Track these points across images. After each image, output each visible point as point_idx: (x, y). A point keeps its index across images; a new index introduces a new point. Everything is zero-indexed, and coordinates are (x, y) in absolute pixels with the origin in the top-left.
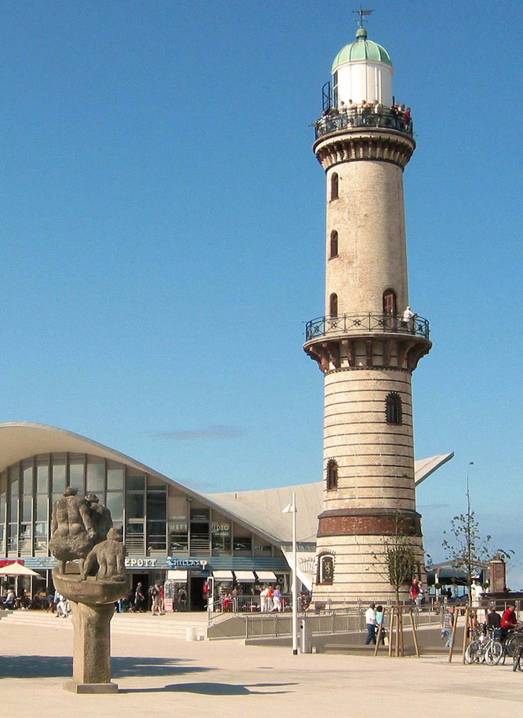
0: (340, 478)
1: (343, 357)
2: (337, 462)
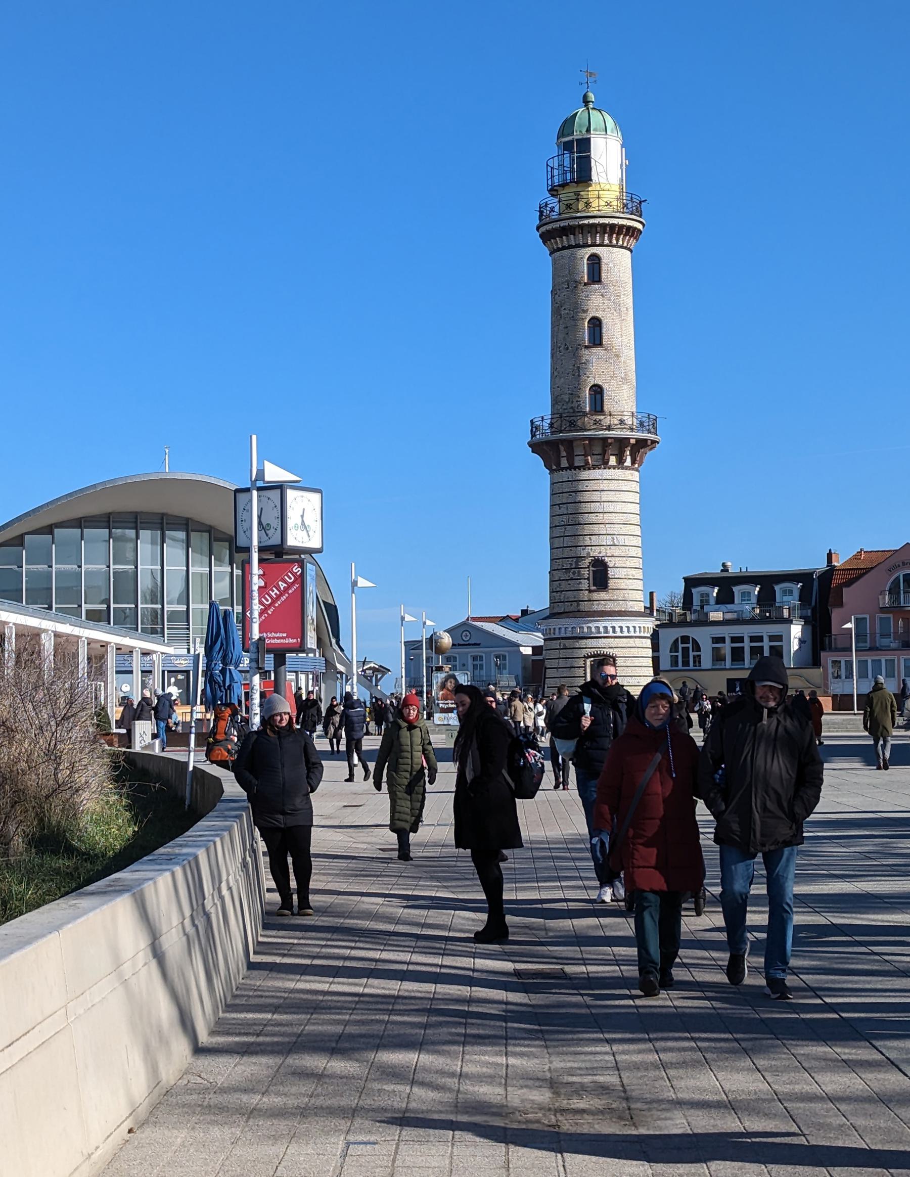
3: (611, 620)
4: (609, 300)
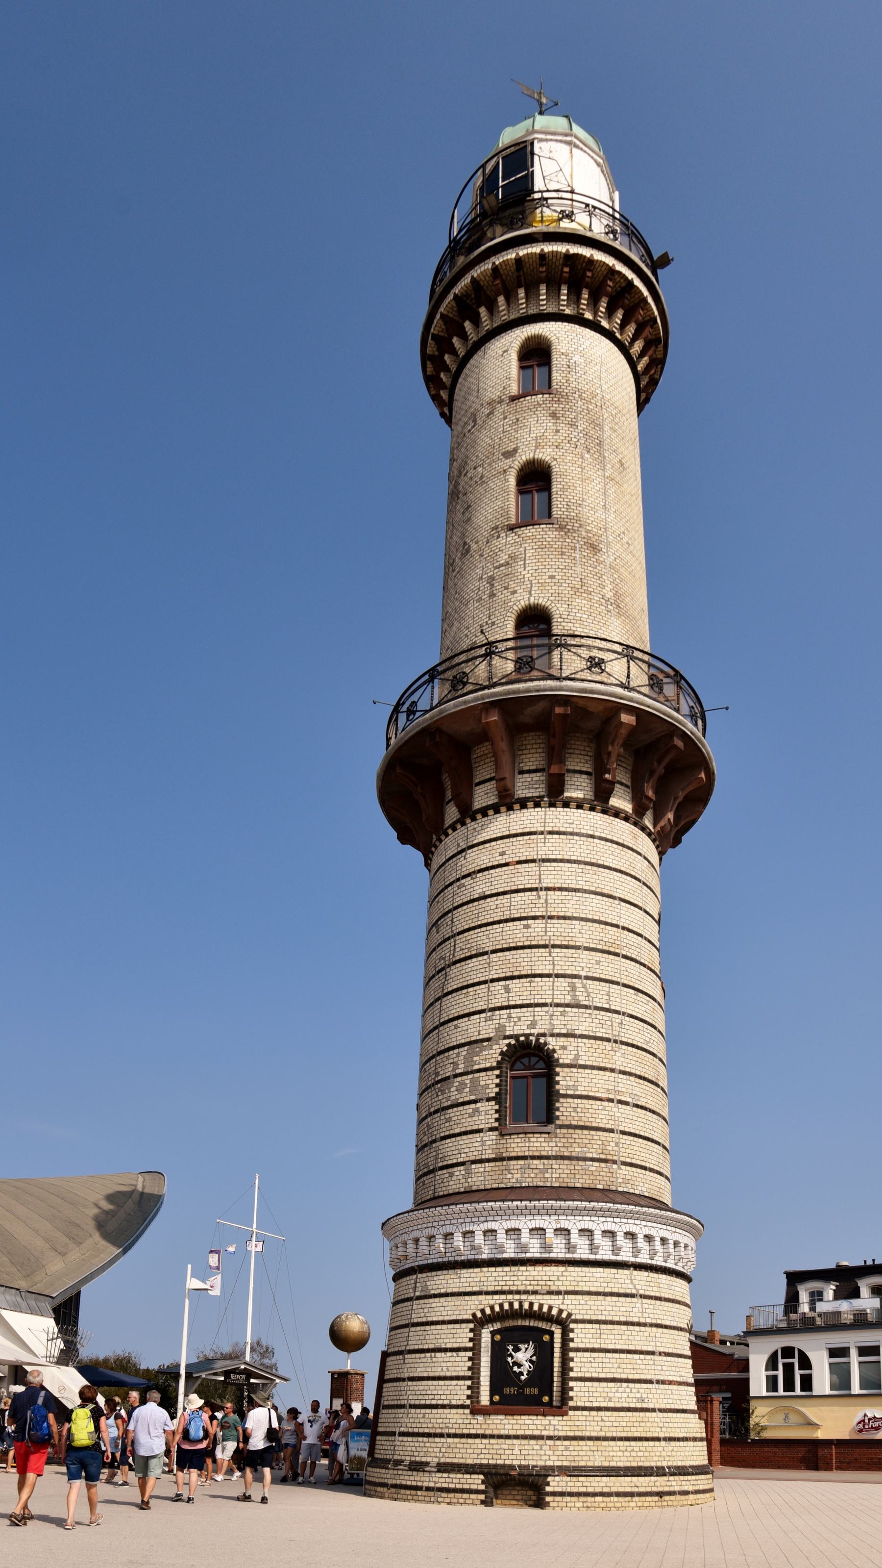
0: (566, 1096)
2: (554, 1051)
3: (556, 1211)
4: (572, 425)
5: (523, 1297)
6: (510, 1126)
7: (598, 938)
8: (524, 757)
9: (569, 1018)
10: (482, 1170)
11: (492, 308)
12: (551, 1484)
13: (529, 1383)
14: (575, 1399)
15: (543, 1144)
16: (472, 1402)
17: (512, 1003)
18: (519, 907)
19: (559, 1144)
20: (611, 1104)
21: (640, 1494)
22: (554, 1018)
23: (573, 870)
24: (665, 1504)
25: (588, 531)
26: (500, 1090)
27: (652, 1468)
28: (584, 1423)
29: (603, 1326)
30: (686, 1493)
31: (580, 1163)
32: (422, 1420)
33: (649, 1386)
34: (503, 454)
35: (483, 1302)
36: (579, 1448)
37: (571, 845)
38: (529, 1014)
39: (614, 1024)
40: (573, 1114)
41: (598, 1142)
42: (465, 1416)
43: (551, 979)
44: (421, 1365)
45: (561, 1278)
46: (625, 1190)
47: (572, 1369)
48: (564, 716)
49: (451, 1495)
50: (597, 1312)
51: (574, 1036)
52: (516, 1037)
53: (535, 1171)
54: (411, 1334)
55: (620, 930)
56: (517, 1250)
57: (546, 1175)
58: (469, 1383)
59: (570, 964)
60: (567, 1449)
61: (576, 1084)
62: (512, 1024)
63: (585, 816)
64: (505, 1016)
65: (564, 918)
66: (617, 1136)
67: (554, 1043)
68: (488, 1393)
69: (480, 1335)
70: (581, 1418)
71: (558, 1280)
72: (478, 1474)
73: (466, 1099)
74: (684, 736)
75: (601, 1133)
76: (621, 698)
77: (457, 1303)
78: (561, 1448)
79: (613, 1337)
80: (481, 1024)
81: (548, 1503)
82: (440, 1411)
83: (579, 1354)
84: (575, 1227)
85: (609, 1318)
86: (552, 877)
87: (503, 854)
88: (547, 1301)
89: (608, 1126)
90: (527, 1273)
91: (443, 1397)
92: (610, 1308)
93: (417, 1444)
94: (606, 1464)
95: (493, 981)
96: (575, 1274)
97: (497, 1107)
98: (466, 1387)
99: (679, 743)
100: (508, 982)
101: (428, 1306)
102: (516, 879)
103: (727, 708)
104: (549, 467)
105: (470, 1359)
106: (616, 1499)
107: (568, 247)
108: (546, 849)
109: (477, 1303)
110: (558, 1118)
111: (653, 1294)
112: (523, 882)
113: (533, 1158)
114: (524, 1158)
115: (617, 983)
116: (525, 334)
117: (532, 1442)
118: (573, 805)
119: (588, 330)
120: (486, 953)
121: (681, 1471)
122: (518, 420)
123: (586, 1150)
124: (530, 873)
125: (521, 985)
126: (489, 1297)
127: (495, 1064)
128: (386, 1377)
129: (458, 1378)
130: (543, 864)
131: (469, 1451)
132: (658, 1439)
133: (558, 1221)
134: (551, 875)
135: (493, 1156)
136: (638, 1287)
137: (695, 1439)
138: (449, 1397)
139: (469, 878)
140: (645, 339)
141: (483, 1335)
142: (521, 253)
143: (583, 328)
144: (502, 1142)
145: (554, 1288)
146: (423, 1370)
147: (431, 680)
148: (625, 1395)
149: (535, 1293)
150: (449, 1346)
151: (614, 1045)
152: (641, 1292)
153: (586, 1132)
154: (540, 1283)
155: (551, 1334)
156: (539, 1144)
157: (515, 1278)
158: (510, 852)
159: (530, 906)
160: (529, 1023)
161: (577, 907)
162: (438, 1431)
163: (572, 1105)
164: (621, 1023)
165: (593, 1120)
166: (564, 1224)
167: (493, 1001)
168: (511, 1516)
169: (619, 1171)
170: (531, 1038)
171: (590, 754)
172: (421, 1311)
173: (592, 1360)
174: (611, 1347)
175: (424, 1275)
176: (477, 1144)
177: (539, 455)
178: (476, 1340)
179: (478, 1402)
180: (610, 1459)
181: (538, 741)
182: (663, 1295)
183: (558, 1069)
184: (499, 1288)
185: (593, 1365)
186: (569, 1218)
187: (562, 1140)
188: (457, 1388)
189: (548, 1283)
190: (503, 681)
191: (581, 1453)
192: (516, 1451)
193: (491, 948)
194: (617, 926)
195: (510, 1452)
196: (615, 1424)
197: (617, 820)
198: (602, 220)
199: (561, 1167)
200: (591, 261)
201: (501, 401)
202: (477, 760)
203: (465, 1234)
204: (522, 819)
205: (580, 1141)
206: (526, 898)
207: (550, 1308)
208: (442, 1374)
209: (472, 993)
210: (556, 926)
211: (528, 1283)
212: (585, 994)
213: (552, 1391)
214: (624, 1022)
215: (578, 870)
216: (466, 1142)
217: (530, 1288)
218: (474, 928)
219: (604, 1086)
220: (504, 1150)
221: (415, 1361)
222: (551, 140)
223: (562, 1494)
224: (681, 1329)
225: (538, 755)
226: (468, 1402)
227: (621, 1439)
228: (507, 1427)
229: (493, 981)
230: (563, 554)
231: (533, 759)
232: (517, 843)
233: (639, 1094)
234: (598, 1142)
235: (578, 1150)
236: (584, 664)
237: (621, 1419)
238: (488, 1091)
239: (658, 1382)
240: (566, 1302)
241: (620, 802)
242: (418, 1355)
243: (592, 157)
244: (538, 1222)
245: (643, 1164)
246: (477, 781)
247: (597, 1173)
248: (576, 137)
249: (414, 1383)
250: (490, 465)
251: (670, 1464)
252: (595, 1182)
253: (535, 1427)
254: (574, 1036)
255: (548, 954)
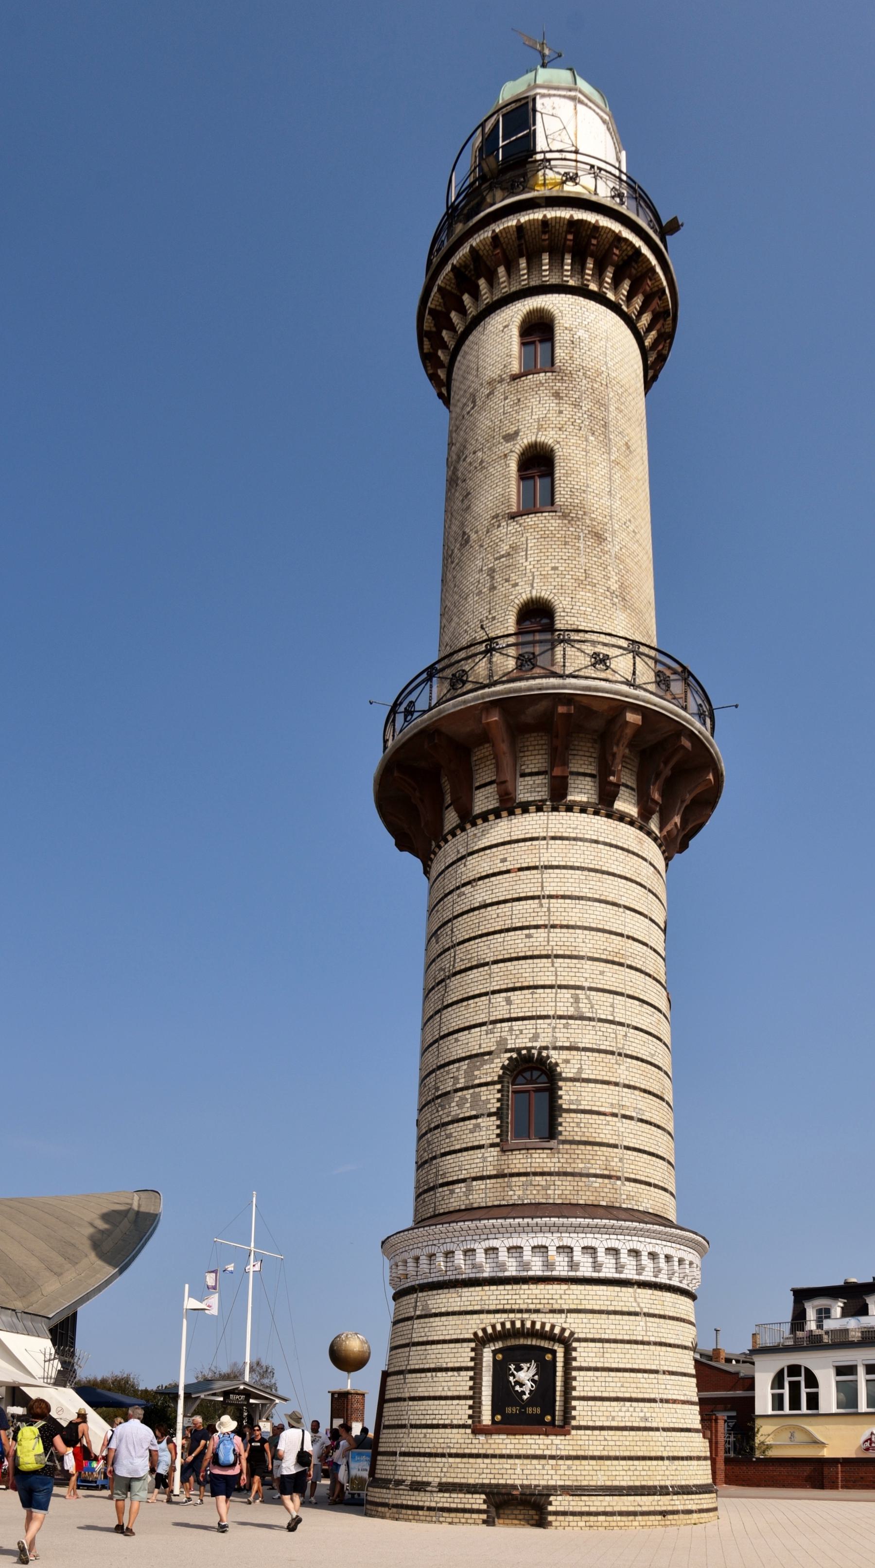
0: (569, 1111)
1: (579, 774)
2: (557, 1064)
3: (559, 1229)
4: (576, 405)
5: (525, 1316)
6: (512, 1142)
7: (602, 947)
8: (526, 758)
9: (572, 1031)
10: (483, 1187)
11: (492, 280)
12: (554, 1503)
13: (531, 1402)
14: (577, 1418)
15: (546, 1160)
16: (473, 1422)
17: (513, 1015)
18: (521, 916)
19: (562, 1160)
20: (615, 1119)
21: (643, 1514)
22: (557, 1030)
23: (576, 877)
24: (668, 1523)
25: (592, 519)
26: (502, 1105)
27: (655, 1487)
28: (587, 1443)
29: (607, 1345)
30: (690, 1512)
31: (584, 1179)
32: (423, 1440)
33: (653, 1405)
34: (504, 438)
35: (485, 1321)
36: (582, 1468)
37: (574, 851)
38: (531, 1027)
39: (619, 1037)
40: (576, 1129)
41: (602, 1158)
42: (466, 1436)
43: (554, 991)
44: (422, 1385)
45: (563, 1297)
46: (629, 1206)
47: (574, 1389)
48: (568, 716)
49: (453, 1515)
50: (600, 1331)
51: (577, 1049)
52: (518, 1050)
53: (537, 1188)
54: (411, 1353)
55: (625, 939)
56: (519, 1268)
57: (549, 1192)
58: (470, 1402)
59: (573, 974)
60: (569, 1468)
61: (579, 1098)
62: (514, 1037)
63: (589, 820)
64: (507, 1029)
65: (568, 927)
66: (621, 1151)
67: (557, 1057)
68: (490, 1413)
69: (482, 1355)
70: (583, 1438)
71: (561, 1298)
72: (480, 1493)
73: (467, 1114)
74: (692, 736)
75: (604, 1149)
76: (626, 697)
77: (458, 1322)
78: (563, 1467)
79: (616, 1356)
80: (482, 1037)
81: (551, 1522)
82: (442, 1431)
83: (582, 1373)
84: (577, 1244)
85: (613, 1337)
86: (555, 884)
87: (504, 860)
88: (549, 1320)
89: (612, 1142)
90: (530, 1292)
91: (444, 1417)
92: (613, 1327)
93: (418, 1464)
94: (609, 1483)
95: (494, 992)
96: (578, 1292)
97: (498, 1122)
98: (467, 1407)
99: (686, 743)
100: (509, 994)
101: (429, 1325)
102: (517, 887)
103: (736, 706)
104: (552, 450)
105: (471, 1378)
106: (619, 1518)
107: (572, 212)
108: (549, 855)
109: (478, 1321)
110: (560, 1133)
111: (657, 1312)
112: (525, 890)
113: (535, 1174)
114: (526, 1174)
115: (622, 994)
116: (527, 308)
117: (535, 1462)
118: (577, 808)
119: (593, 303)
120: (487, 964)
121: (685, 1490)
122: (519, 400)
123: (589, 1165)
124: (533, 881)
125: (522, 997)
126: (491, 1316)
127: (496, 1078)
128: (387, 1397)
129: (459, 1398)
130: (545, 871)
131: (470, 1470)
132: (662, 1458)
133: (560, 1238)
134: (554, 883)
135: (495, 1172)
136: (642, 1305)
137: (699, 1458)
138: (451, 1417)
139: (469, 886)
140: (653, 312)
141: (485, 1354)
142: (523, 220)
143: (588, 301)
144: (503, 1158)
145: (556, 1307)
146: (424, 1389)
147: (429, 679)
148: (628, 1414)
149: (537, 1311)
150: (450, 1365)
151: (618, 1058)
152: (645, 1310)
153: (589, 1148)
154: (542, 1301)
155: (554, 1352)
156: (541, 1160)
157: (517, 1297)
158: (512, 859)
159: (532, 914)
160: (531, 1035)
161: (581, 915)
162: (440, 1451)
163: (576, 1120)
164: (626, 1036)
165: (596, 1135)
166: (566, 1242)
167: (495, 1013)
168: (513, 1537)
169: (623, 1188)
170: (533, 1051)
171: (594, 755)
172: (422, 1330)
173: (595, 1379)
174: (614, 1365)
175: (425, 1294)
176: (478, 1161)
177: (542, 438)
178: (477, 1359)
179: (480, 1422)
180: (613, 1478)
181: (540, 742)
182: (667, 1313)
183: (560, 1084)
184: (501, 1307)
185: (596, 1384)
186: (572, 1235)
187: (565, 1156)
188: (458, 1407)
189: (551, 1301)
190: (505, 679)
191: (584, 1473)
192: (519, 1471)
193: (492, 959)
194: (622, 935)
195: (512, 1471)
196: (618, 1443)
197: (622, 824)
198: (608, 182)
199: (564, 1183)
200: (596, 228)
201: (501, 381)
202: (477, 763)
203: (466, 1252)
204: (524, 824)
205: (583, 1157)
206: (528, 906)
207: (553, 1327)
208: (444, 1394)
209: (472, 1006)
210: (559, 935)
211: (530, 1301)
212: (589, 1006)
213: (554, 1410)
214: (629, 1035)
215: (582, 877)
216: (467, 1158)
217: (532, 1307)
218: (474, 938)
219: (608, 1100)
220: (506, 1166)
221: (415, 1380)
222: (554, 95)
223: (564, 1513)
224: (685, 1348)
225: (540, 757)
226: (470, 1422)
227: (624, 1458)
228: (509, 1446)
229: (494, 992)
230: (566, 543)
231: (535, 761)
232: (519, 849)
233: (644, 1108)
234: (602, 1158)
235: (581, 1165)
236: (587, 661)
237: (624, 1438)
238: (489, 1106)
239: (662, 1401)
240: (569, 1320)
241: (625, 805)
242: (419, 1375)
243: (598, 114)
244: (540, 1240)
245: (647, 1180)
246: (477, 784)
247: (600, 1190)
248: (581, 92)
249: (415, 1403)
250: (490, 449)
251: (674, 1483)
252: (598, 1198)
253: (536, 1447)
254: (577, 1049)
255: (550, 965)
